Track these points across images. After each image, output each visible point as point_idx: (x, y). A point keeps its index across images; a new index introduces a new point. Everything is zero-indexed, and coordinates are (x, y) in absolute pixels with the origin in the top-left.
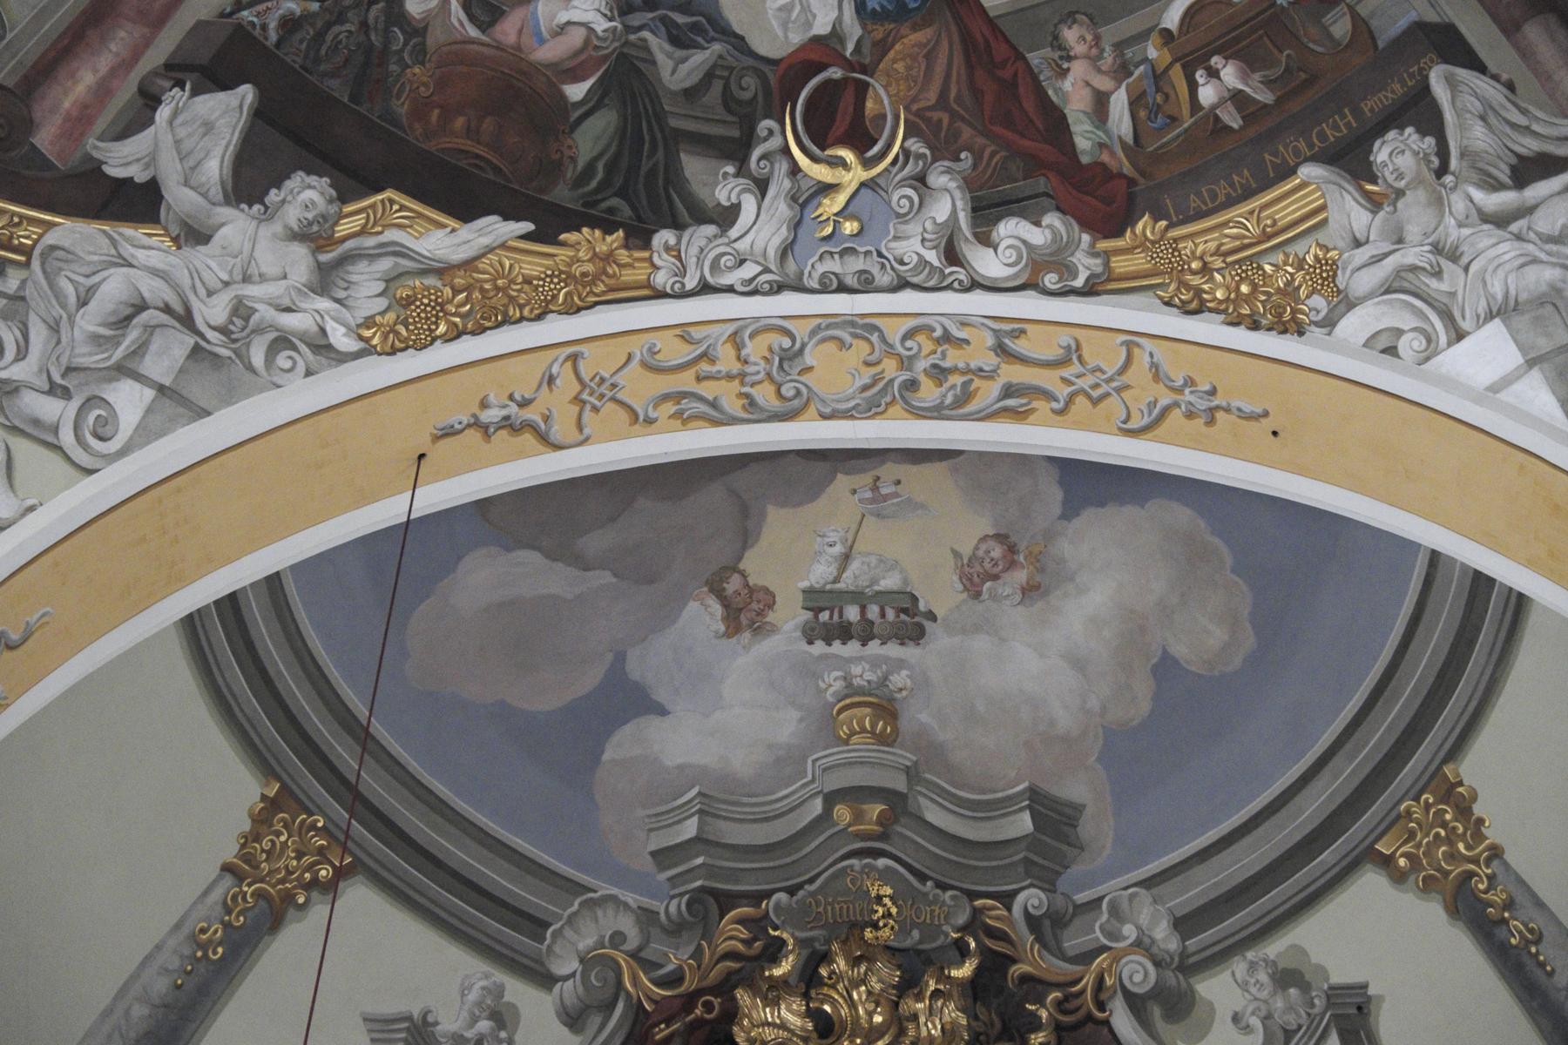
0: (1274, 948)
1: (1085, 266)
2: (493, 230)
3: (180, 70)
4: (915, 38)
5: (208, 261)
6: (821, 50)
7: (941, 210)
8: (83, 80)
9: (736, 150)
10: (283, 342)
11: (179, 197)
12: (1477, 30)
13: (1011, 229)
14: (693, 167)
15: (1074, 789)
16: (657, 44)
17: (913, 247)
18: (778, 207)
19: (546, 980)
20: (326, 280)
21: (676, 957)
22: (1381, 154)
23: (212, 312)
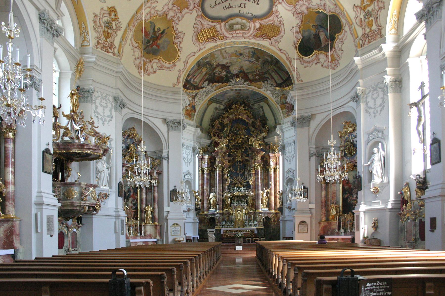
0: (259, 103)
1: (250, 84)
2: (220, 84)
3: (205, 81)
4: (241, 73)
5: (207, 89)
6: (237, 74)
7: (243, 81)
8: (201, 83)
9: (232, 78)
10: (210, 91)
11: (205, 86)
12: (270, 78)
13: (246, 82)
14: (230, 80)
15: (248, 96)
16: (228, 74)
17: (241, 83)
18: (234, 81)
19: (221, 104)
20: (212, 88)
21: (228, 103)
22: (265, 82)
23: (207, 91)
